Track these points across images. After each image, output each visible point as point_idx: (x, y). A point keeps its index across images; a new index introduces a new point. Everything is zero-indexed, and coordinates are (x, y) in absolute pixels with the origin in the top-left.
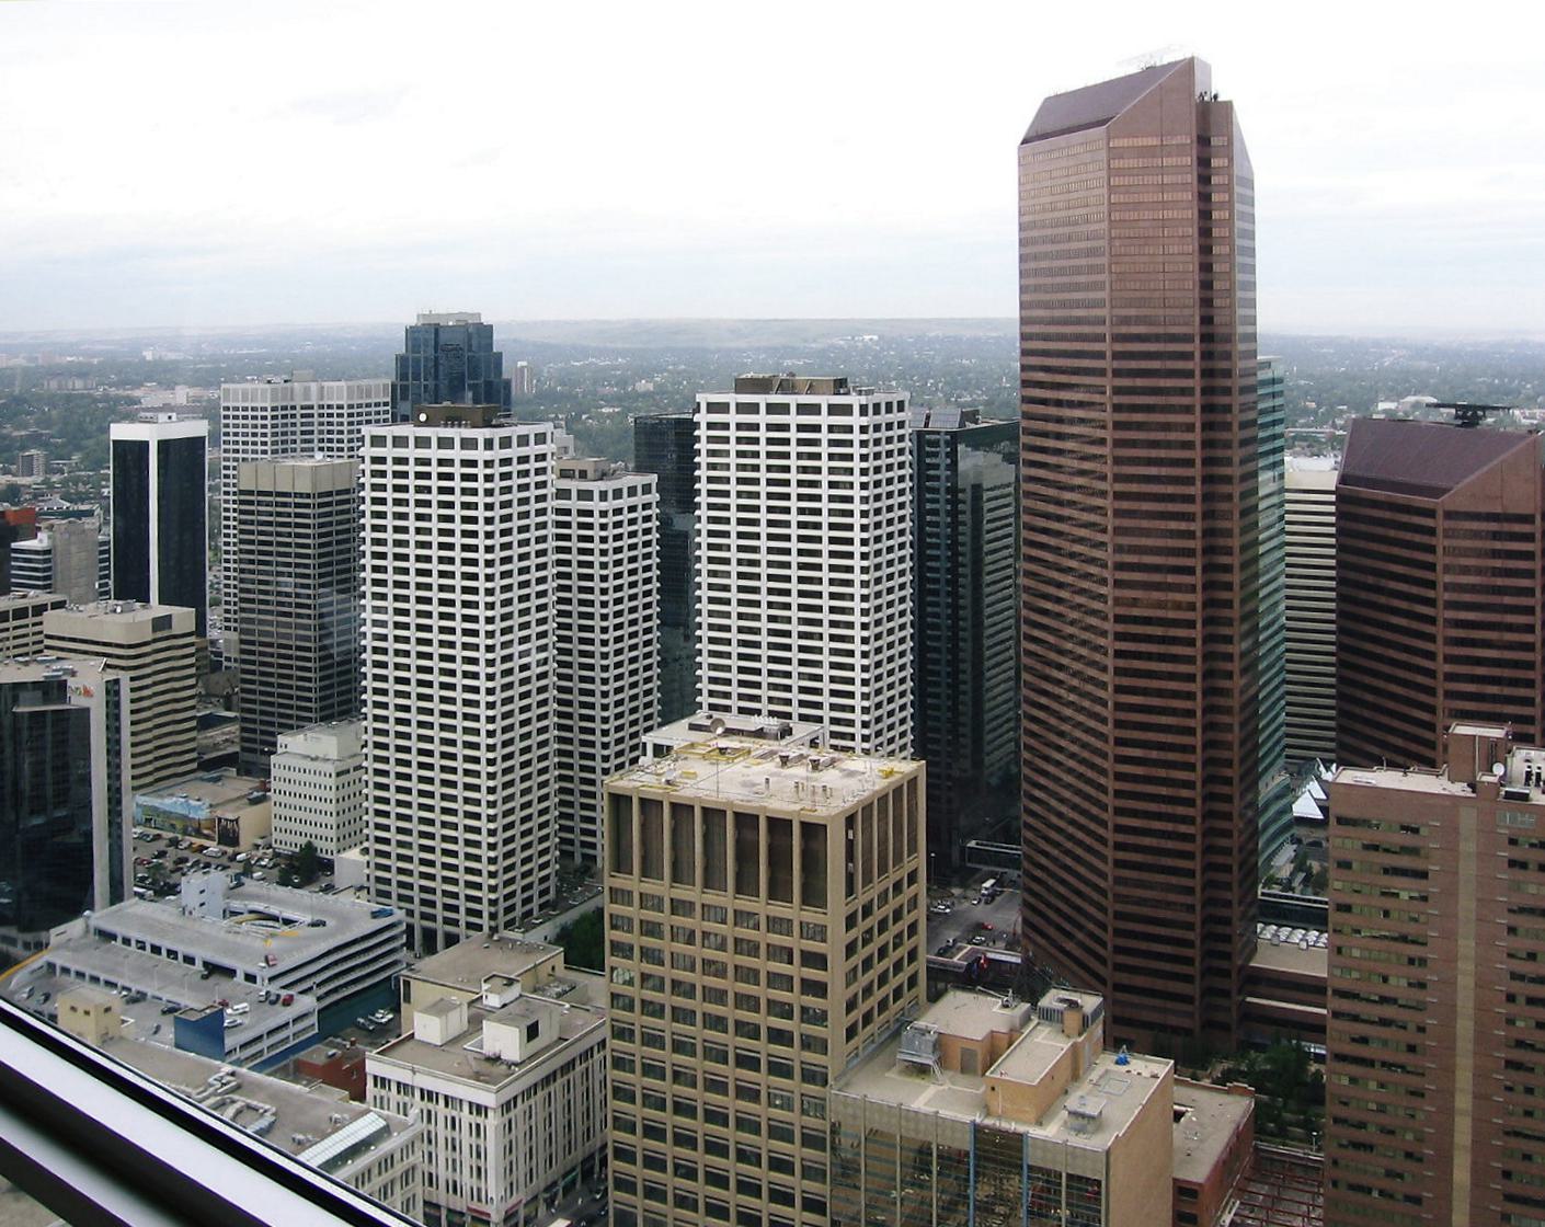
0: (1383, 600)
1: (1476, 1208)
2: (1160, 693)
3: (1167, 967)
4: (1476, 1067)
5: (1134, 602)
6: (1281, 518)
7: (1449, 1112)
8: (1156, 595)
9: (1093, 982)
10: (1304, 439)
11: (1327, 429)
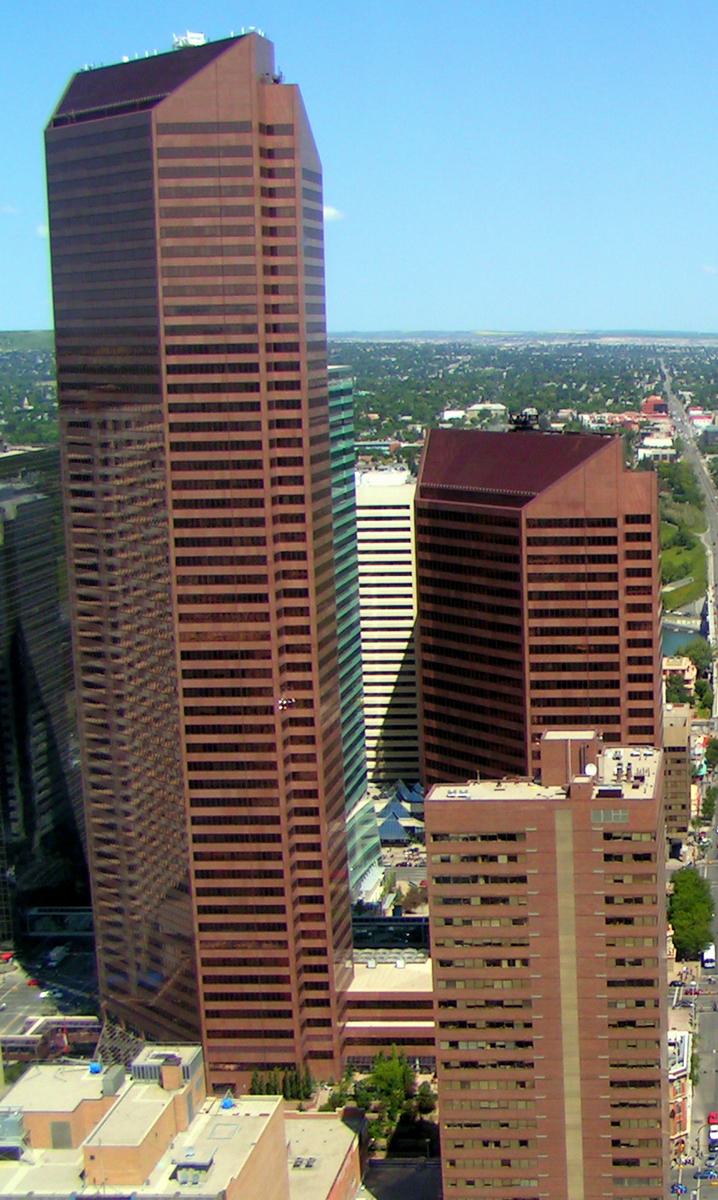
0: (466, 613)
1: (589, 1180)
2: (237, 729)
3: (264, 1005)
4: (581, 1052)
5: (200, 637)
6: (354, 536)
7: (558, 1097)
8: (226, 627)
9: (185, 1032)
10: (368, 453)
11: (390, 441)
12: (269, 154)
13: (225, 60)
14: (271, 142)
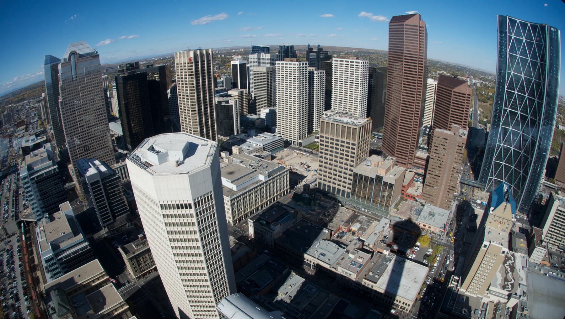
12: (420, 30)
13: (415, 16)
14: (421, 29)
